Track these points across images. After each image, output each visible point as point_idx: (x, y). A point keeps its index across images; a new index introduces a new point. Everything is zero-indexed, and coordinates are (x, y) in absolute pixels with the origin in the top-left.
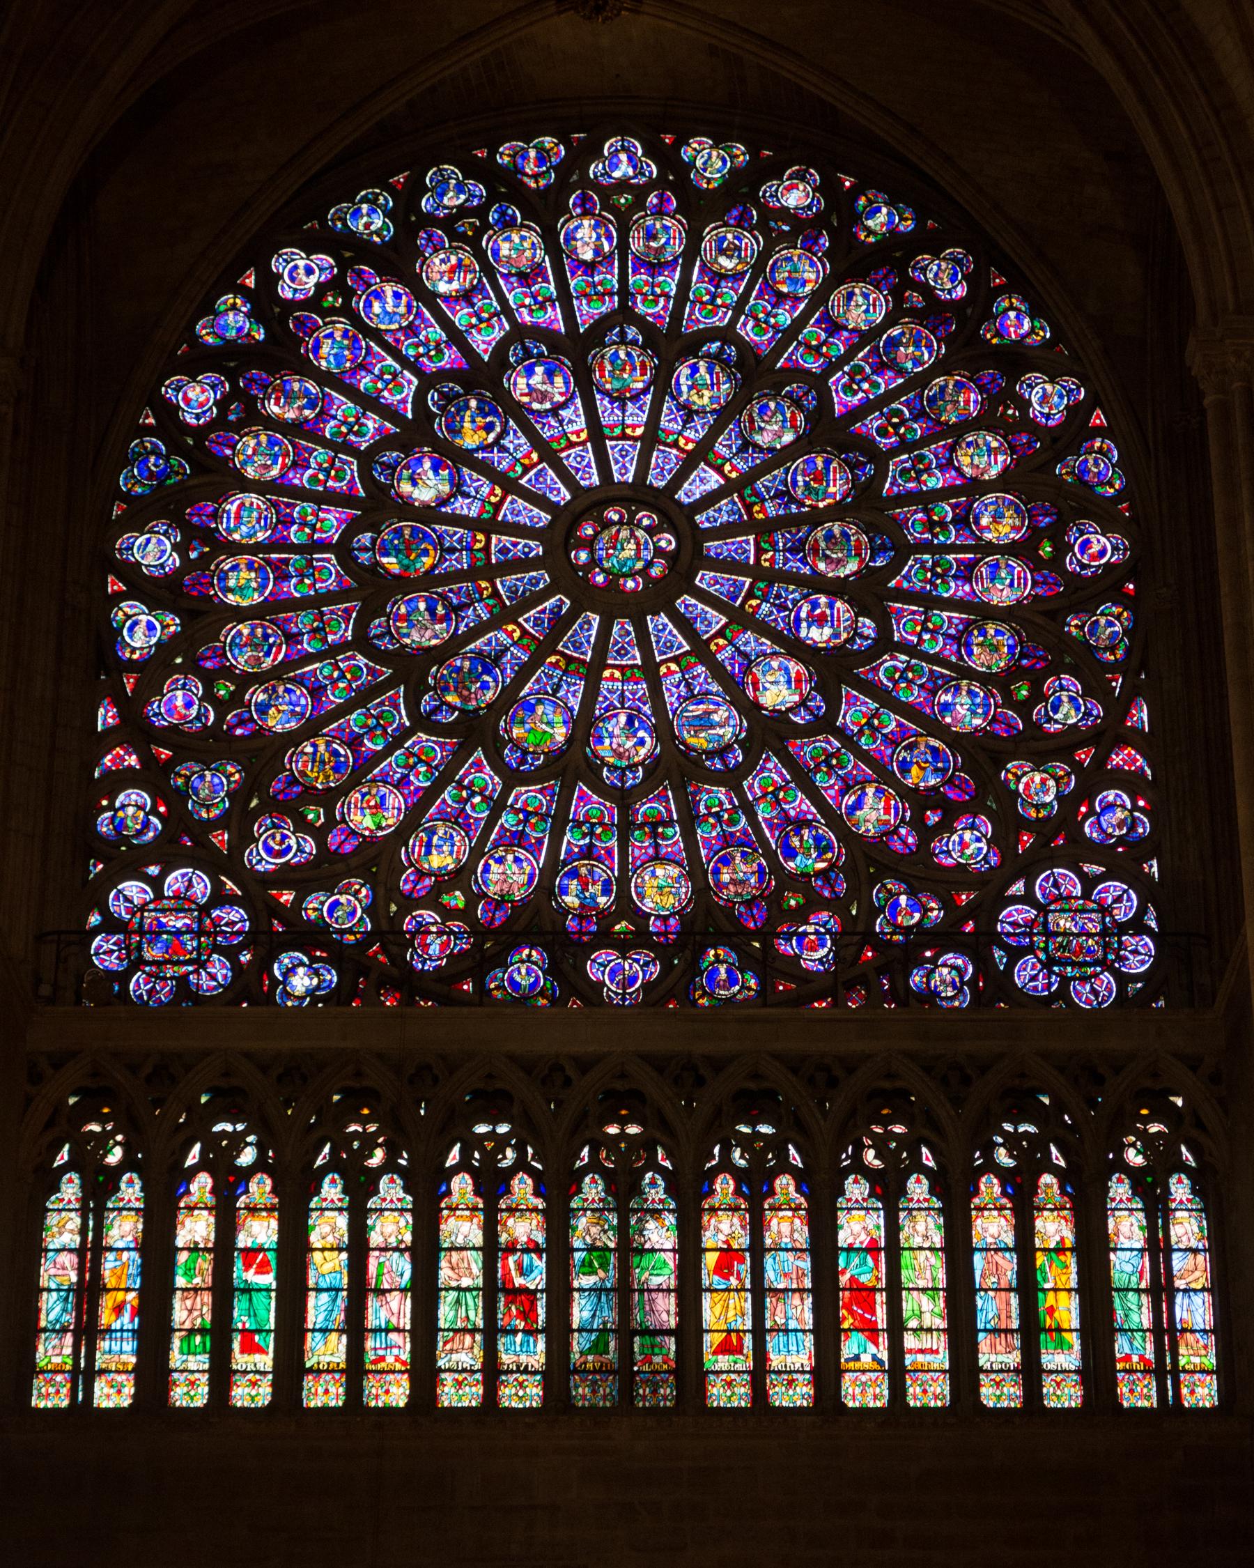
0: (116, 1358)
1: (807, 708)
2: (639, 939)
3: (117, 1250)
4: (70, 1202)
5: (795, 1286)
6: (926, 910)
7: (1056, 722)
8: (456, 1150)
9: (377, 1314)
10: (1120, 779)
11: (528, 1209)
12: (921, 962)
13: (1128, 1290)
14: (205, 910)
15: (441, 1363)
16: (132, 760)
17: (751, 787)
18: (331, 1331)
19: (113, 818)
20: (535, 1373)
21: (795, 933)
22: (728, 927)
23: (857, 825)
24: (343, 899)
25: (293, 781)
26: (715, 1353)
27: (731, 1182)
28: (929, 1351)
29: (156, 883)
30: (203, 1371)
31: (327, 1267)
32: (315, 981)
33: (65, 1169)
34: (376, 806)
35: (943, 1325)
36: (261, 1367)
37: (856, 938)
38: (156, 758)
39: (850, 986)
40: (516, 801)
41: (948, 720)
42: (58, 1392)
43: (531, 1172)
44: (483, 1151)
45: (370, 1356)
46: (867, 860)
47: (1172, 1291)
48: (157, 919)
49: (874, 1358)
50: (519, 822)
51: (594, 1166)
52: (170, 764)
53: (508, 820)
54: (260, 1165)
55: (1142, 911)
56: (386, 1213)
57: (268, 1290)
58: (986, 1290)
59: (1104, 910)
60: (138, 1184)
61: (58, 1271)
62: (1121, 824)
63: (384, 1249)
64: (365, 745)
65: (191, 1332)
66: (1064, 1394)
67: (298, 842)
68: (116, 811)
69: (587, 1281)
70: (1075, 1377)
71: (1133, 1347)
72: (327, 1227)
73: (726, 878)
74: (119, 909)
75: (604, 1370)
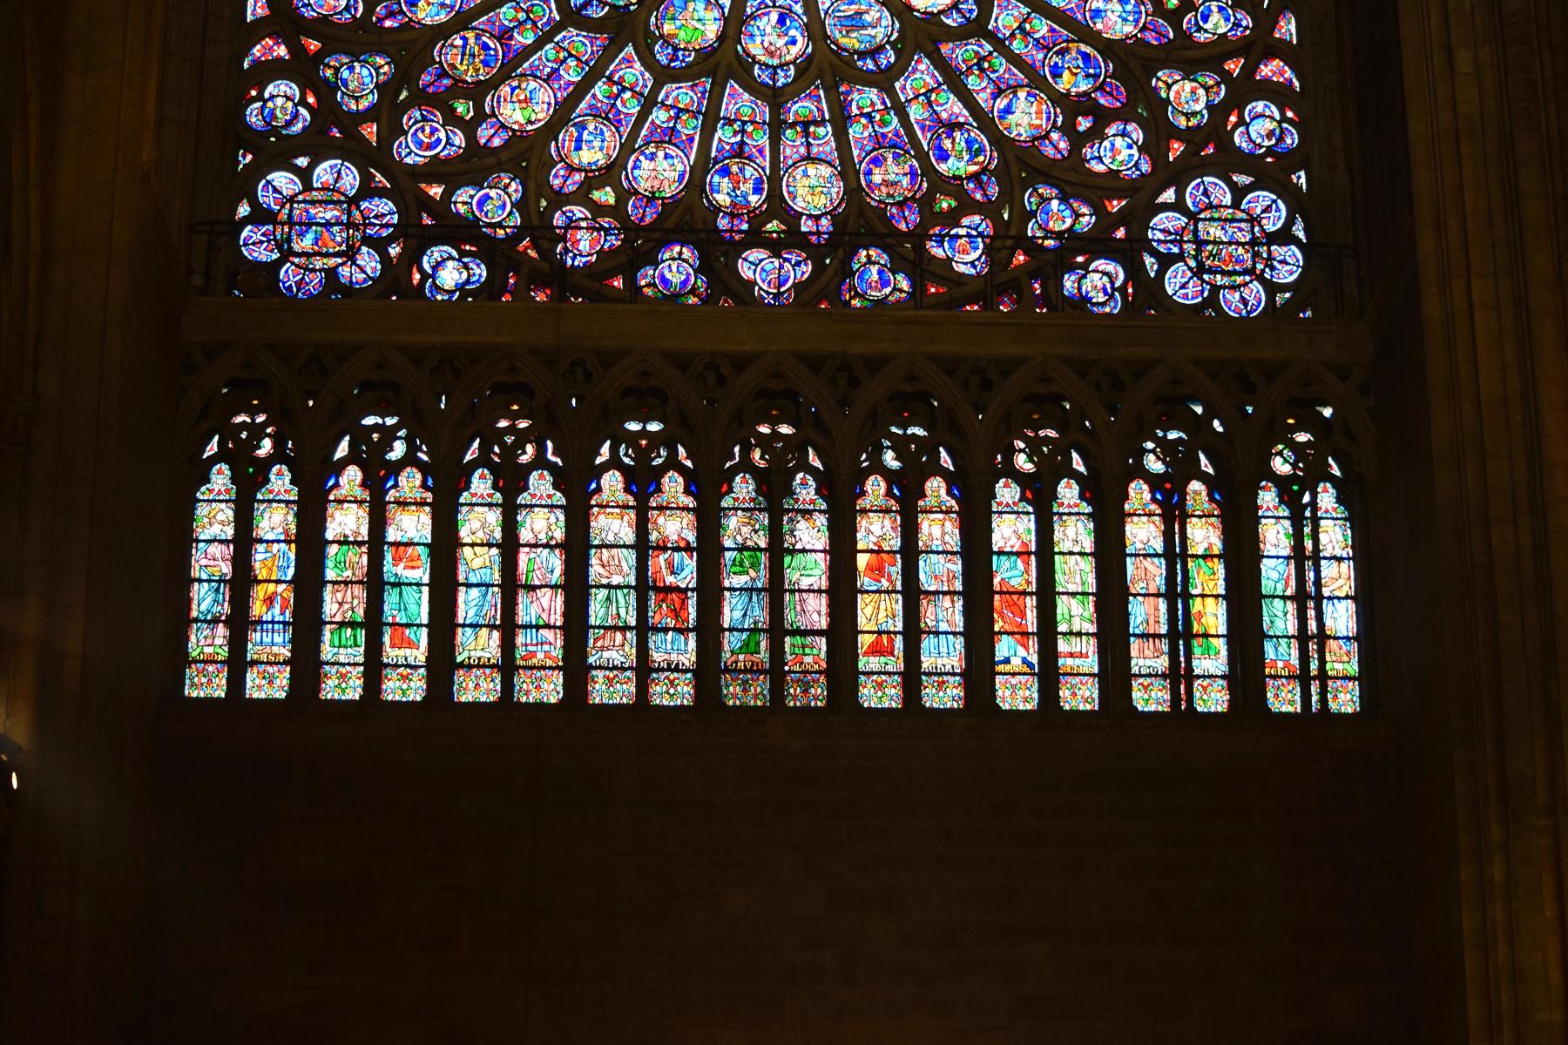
0: (268, 650)
1: (959, 11)
2: (793, 239)
3: (267, 542)
4: (219, 493)
5: (945, 588)
6: (1077, 216)
7: (1206, 31)
8: (605, 449)
9: (527, 609)
10: (1270, 91)
11: (678, 508)
12: (1072, 268)
13: (1274, 597)
14: (354, 201)
15: (591, 660)
16: (282, 51)
17: (903, 88)
18: (482, 626)
19: (263, 108)
20: (686, 671)
21: (947, 234)
22: (881, 228)
23: (1008, 128)
24: (493, 193)
25: (443, 74)
26: (866, 654)
27: (883, 484)
28: (1080, 655)
29: (305, 175)
30: (355, 664)
31: (478, 563)
32: (465, 275)
33: (214, 460)
34: (525, 100)
35: (1092, 629)
36: (411, 661)
37: (1009, 242)
38: (305, 50)
39: (1002, 290)
40: (667, 97)
41: (1099, 26)
42: (210, 681)
43: (682, 470)
44: (637, 448)
45: (520, 653)
46: (1019, 165)
47: (1319, 598)
48: (307, 211)
49: (1024, 661)
50: (668, 121)
51: (746, 466)
52: (319, 57)
53: (660, 116)
54: (409, 460)
55: (1290, 222)
56: (536, 510)
57: (418, 585)
58: (1135, 595)
59: (1253, 220)
60: (288, 477)
61: (210, 561)
62: (1270, 134)
63: (535, 546)
64: (511, 38)
65: (342, 624)
66: (1213, 699)
67: (448, 137)
68: (265, 101)
69: (739, 581)
70: (1220, 682)
71: (1280, 654)
72: (479, 522)
73: (877, 178)
74: (266, 199)
75: (754, 670)
